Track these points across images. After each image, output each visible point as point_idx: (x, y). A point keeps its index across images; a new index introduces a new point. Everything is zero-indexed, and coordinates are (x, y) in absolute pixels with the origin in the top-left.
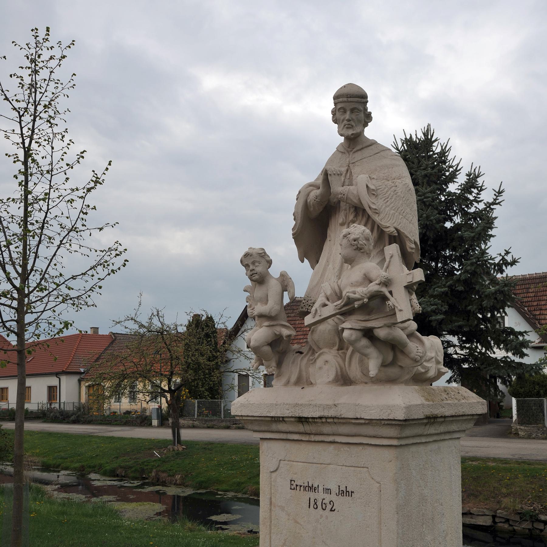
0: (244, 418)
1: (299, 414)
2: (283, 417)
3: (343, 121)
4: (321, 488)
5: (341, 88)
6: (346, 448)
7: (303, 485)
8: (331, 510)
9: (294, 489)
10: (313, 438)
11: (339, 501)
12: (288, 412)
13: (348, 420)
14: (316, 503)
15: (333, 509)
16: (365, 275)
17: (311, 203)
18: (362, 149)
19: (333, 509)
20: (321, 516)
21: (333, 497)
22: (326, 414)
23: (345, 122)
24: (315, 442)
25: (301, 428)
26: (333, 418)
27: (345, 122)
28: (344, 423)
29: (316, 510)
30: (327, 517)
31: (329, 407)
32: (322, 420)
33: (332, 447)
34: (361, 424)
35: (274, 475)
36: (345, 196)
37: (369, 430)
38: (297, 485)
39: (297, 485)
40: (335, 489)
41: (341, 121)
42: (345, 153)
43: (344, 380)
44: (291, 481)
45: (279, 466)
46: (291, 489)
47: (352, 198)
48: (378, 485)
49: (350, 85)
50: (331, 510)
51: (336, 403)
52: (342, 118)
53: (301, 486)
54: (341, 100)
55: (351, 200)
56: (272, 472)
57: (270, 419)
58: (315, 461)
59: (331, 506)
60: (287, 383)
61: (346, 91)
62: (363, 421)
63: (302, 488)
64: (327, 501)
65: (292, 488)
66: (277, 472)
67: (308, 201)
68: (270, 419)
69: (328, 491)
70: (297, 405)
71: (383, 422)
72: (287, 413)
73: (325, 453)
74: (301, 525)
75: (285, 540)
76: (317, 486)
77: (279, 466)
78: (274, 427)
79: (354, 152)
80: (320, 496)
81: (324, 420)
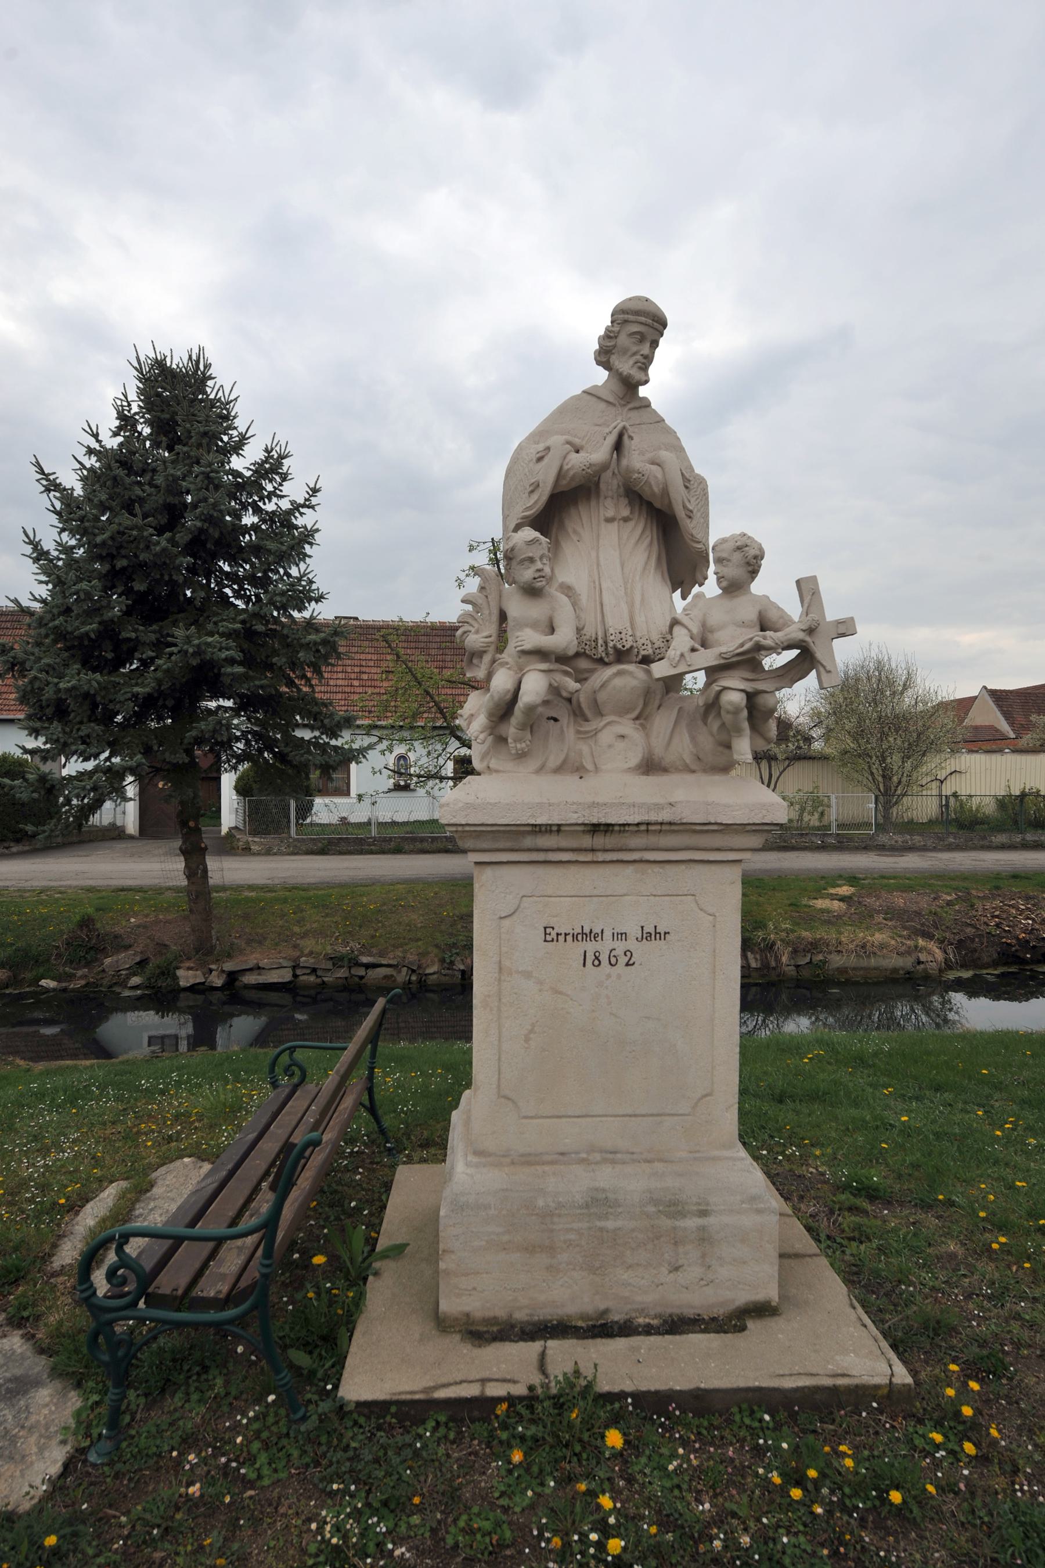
0: (467, 828)
1: (599, 818)
2: (559, 825)
3: (634, 354)
4: (608, 934)
5: (630, 299)
6: (657, 868)
7: (571, 932)
8: (627, 965)
9: (553, 940)
10: (601, 856)
11: (640, 950)
12: (575, 816)
13: (688, 827)
14: (597, 958)
15: (631, 962)
16: (760, 613)
17: (571, 473)
18: (640, 407)
19: (631, 962)
20: (609, 976)
21: (631, 944)
22: (653, 817)
23: (638, 357)
24: (603, 862)
25: (587, 841)
26: (661, 824)
27: (638, 357)
28: (674, 831)
29: (599, 968)
30: (619, 976)
31: (659, 807)
32: (645, 827)
33: (630, 869)
34: (713, 831)
35: (506, 923)
36: (645, 478)
37: (718, 841)
38: (558, 934)
39: (558, 934)
40: (634, 932)
41: (629, 353)
42: (614, 405)
43: (650, 766)
44: (545, 928)
45: (519, 906)
46: (545, 941)
47: (653, 483)
48: (711, 918)
49: (639, 299)
50: (627, 965)
51: (672, 800)
52: (635, 349)
53: (566, 935)
54: (643, 319)
55: (651, 486)
56: (501, 918)
57: (529, 829)
58: (596, 892)
59: (627, 959)
60: (540, 770)
61: (633, 306)
62: (715, 827)
63: (569, 938)
64: (619, 952)
65: (549, 938)
66: (515, 917)
67: (566, 467)
68: (529, 829)
69: (623, 936)
70: (594, 805)
71: (748, 828)
72: (574, 818)
73: (621, 879)
74: (568, 996)
75: (533, 1025)
76: (599, 932)
77: (519, 906)
78: (528, 842)
79: (630, 409)
80: (604, 946)
81: (643, 828)
